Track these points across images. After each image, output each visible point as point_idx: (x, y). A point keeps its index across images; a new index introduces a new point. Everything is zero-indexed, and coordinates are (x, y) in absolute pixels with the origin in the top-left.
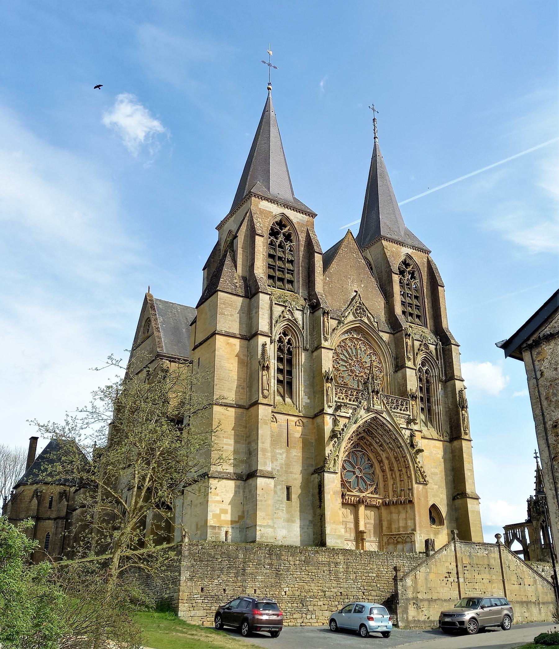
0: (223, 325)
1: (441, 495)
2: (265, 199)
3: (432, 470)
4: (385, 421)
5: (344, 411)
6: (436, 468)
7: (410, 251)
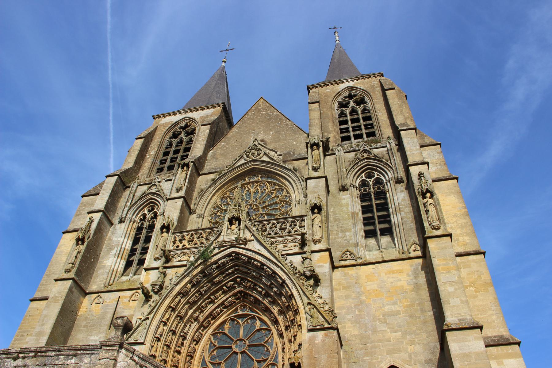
0: (76, 224)
1: (409, 347)
2: (167, 116)
3: (386, 309)
4: (249, 254)
5: (180, 259)
6: (395, 303)
7: (351, 84)
